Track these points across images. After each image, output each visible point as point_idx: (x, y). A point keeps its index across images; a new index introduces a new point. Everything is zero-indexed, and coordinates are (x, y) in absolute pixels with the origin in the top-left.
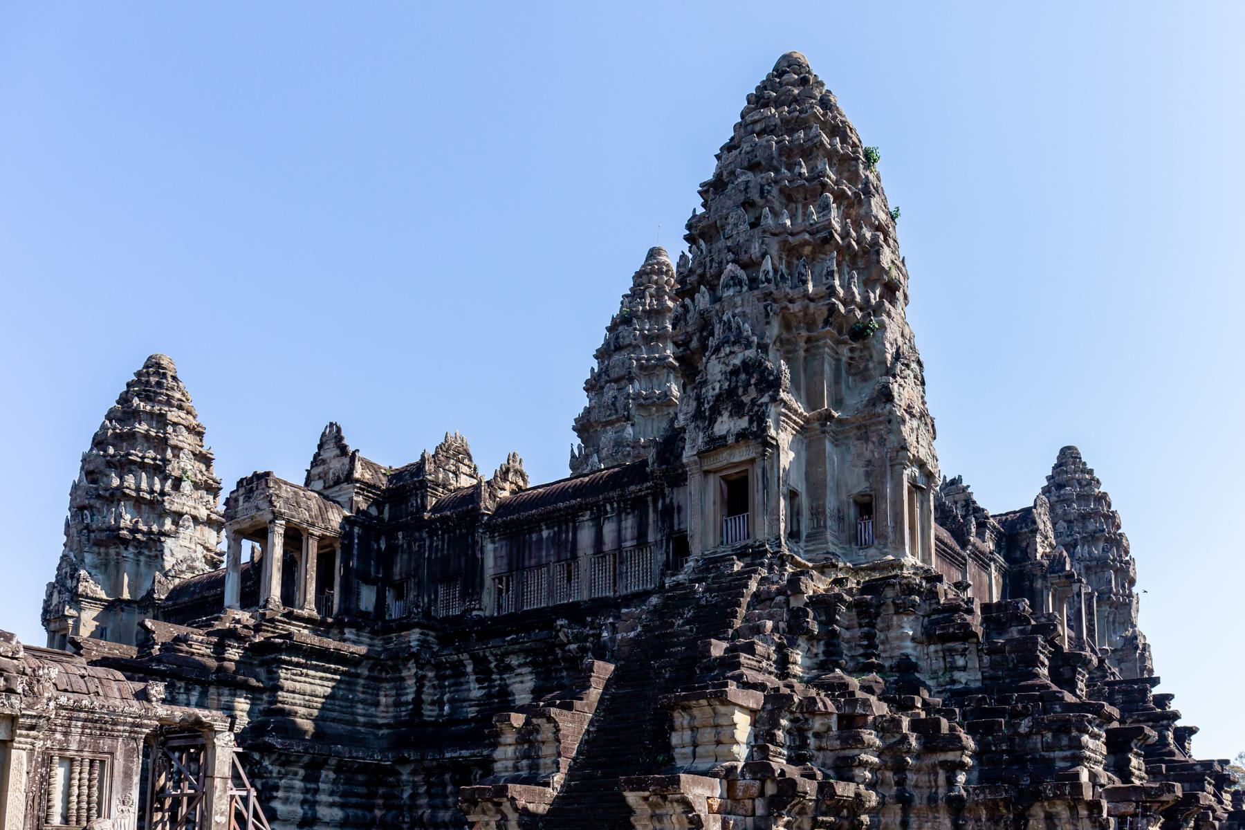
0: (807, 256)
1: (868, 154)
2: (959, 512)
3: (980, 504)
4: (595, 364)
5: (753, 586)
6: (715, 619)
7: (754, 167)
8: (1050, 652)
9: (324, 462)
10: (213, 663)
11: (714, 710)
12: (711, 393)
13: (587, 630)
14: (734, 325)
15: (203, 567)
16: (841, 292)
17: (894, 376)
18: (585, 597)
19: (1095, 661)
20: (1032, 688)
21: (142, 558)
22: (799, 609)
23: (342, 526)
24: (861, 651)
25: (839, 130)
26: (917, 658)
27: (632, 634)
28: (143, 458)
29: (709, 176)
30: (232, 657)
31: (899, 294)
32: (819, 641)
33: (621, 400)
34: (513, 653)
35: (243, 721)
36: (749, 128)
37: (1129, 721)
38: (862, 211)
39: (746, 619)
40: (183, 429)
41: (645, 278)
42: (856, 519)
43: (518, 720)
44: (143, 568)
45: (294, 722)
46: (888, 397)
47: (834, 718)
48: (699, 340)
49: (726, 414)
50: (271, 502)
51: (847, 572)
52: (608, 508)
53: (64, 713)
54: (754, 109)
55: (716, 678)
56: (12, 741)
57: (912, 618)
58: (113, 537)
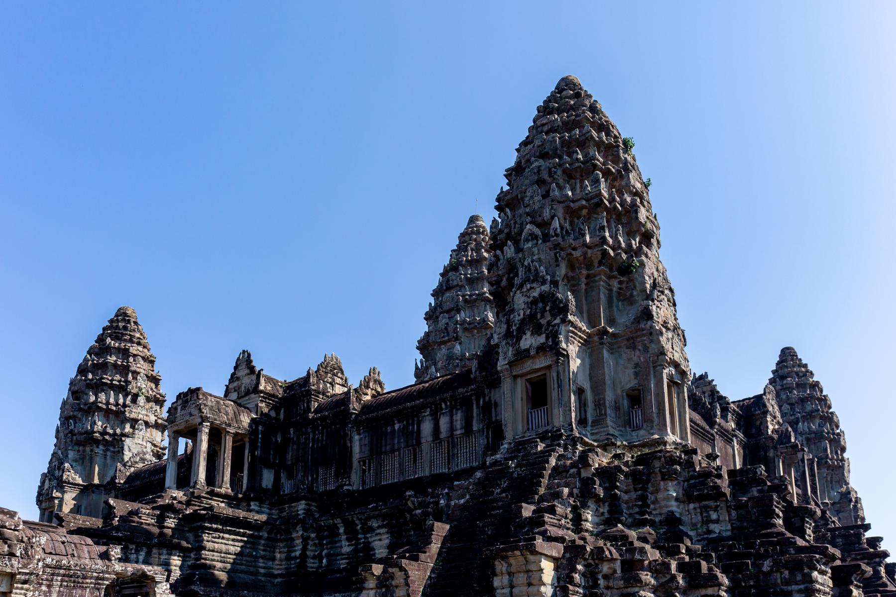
0: (584, 216)
1: (625, 143)
2: (707, 400)
3: (723, 393)
4: (432, 301)
5: (553, 461)
6: (525, 488)
7: (544, 156)
8: (783, 506)
9: (238, 379)
10: (156, 530)
11: (525, 558)
12: (517, 318)
13: (428, 499)
14: (532, 268)
15: (151, 458)
16: (610, 241)
17: (653, 301)
18: (427, 473)
19: (819, 513)
20: (771, 535)
21: (109, 453)
22: (588, 478)
23: (250, 425)
24: (637, 510)
25: (604, 127)
26: (681, 514)
27: (462, 501)
28: (112, 380)
29: (512, 163)
30: (170, 525)
31: (654, 241)
32: (604, 503)
33: (452, 325)
34: (374, 517)
35: (176, 573)
36: (539, 129)
37: (849, 560)
38: (623, 183)
39: (548, 487)
40: (140, 359)
41: (467, 238)
42: (629, 408)
43: (377, 569)
44: (109, 461)
45: (213, 574)
46: (647, 315)
47: (618, 563)
48: (507, 280)
49: (529, 333)
50: (200, 410)
51: (624, 449)
52: (443, 406)
53: (48, 570)
54: (543, 116)
55: (526, 533)
56: (11, 592)
57: (675, 482)
58: (89, 439)
